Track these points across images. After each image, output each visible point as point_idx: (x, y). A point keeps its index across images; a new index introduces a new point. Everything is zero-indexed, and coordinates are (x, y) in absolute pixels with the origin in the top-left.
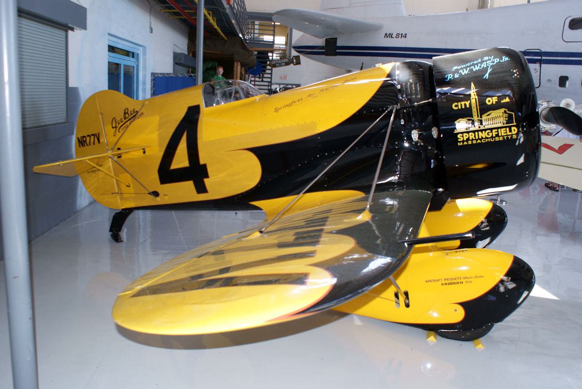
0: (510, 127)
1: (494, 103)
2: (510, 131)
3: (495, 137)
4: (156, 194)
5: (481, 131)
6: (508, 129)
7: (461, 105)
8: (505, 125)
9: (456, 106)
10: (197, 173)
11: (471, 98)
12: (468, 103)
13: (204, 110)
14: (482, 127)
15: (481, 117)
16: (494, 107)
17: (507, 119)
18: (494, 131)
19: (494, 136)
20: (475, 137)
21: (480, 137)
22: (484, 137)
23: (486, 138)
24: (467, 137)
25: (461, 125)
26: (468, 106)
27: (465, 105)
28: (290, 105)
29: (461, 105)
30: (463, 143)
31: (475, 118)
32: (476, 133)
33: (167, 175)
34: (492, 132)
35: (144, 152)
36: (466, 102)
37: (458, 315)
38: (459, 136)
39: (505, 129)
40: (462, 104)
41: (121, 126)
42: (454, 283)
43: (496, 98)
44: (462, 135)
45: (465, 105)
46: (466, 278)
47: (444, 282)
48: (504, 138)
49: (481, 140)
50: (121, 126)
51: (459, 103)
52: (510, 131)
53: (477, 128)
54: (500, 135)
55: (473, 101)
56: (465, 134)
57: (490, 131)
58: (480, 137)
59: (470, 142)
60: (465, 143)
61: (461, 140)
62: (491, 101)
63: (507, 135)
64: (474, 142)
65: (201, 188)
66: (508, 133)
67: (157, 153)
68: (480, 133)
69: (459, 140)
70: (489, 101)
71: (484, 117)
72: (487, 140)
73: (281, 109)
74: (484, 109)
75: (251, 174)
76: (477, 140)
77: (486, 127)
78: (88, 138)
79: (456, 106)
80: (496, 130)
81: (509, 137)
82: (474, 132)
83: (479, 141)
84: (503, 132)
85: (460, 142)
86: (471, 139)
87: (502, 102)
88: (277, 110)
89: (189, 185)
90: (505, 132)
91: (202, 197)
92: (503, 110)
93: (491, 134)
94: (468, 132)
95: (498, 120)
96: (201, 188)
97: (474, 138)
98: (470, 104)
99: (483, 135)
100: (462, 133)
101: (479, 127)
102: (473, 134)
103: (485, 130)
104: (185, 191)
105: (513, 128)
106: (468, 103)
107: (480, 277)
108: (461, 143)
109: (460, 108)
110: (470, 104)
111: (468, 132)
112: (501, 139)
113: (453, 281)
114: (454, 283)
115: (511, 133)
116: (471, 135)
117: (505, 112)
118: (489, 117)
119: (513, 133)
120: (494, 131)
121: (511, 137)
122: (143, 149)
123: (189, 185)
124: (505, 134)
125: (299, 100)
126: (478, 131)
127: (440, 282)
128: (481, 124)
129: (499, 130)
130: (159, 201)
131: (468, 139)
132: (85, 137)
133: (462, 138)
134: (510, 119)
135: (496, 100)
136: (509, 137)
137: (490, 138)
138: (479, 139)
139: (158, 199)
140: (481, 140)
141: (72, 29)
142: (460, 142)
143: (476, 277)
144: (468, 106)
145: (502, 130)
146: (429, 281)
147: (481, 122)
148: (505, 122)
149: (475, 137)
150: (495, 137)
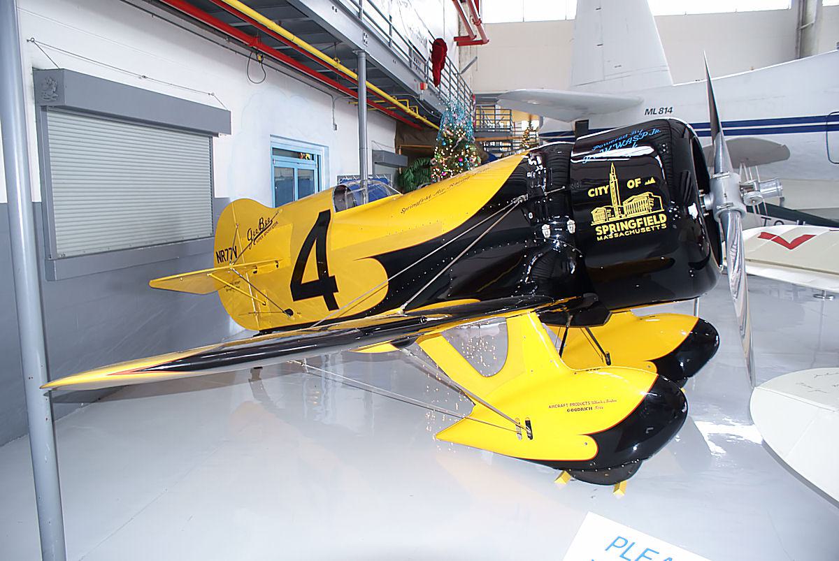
0: (657, 215)
1: (637, 186)
2: (658, 219)
3: (640, 228)
4: (289, 312)
5: (623, 221)
6: (654, 217)
7: (598, 191)
8: (651, 212)
9: (592, 193)
10: (326, 287)
11: (610, 182)
12: (606, 189)
13: (335, 216)
14: (624, 217)
15: (622, 204)
16: (637, 191)
17: (653, 205)
18: (638, 220)
19: (639, 226)
20: (616, 229)
21: (623, 230)
22: (627, 228)
23: (632, 230)
24: (607, 230)
25: (599, 215)
26: (606, 192)
27: (603, 190)
28: (418, 204)
29: (598, 191)
30: (603, 238)
31: (615, 206)
32: (617, 224)
33: (300, 290)
34: (636, 222)
35: (277, 266)
36: (604, 187)
37: (589, 451)
38: (597, 229)
39: (651, 217)
40: (599, 191)
41: (257, 237)
42: (582, 409)
43: (639, 179)
44: (600, 227)
45: (603, 190)
46: (596, 403)
47: (570, 408)
48: (651, 229)
49: (623, 232)
50: (257, 237)
51: (596, 189)
52: (658, 219)
53: (617, 218)
54: (646, 225)
55: (612, 185)
57: (633, 221)
59: (611, 236)
60: (606, 237)
61: (601, 234)
62: (633, 183)
63: (655, 225)
64: (616, 235)
65: (332, 305)
66: (656, 222)
67: (289, 264)
68: (621, 223)
69: (598, 234)
70: (631, 184)
71: (626, 204)
72: (631, 232)
73: (407, 209)
74: (625, 193)
75: (377, 283)
76: (619, 233)
77: (628, 217)
78: (226, 252)
79: (592, 193)
80: (641, 219)
81: (658, 226)
82: (614, 223)
83: (621, 234)
84: (649, 221)
85: (599, 236)
87: (646, 183)
88: (403, 211)
89: (321, 299)
90: (652, 220)
91: (334, 314)
92: (647, 194)
93: (634, 224)
94: (607, 224)
95: (642, 207)
96: (332, 305)
97: (615, 231)
98: (609, 190)
99: (626, 226)
100: (601, 225)
101: (621, 217)
102: (613, 225)
103: (628, 220)
104: (315, 308)
105: (661, 216)
106: (606, 189)
107: (612, 401)
109: (597, 195)
110: (609, 190)
111: (607, 224)
113: (580, 407)
114: (582, 409)
115: (659, 222)
116: (612, 228)
117: (650, 196)
118: (631, 203)
119: (662, 221)
120: (638, 220)
121: (660, 227)
122: (277, 262)
123: (321, 299)
124: (653, 224)
125: (427, 198)
126: (619, 221)
127: (565, 408)
128: (623, 213)
130: (293, 320)
131: (608, 233)
132: (222, 251)
133: (601, 231)
134: (656, 206)
135: (640, 183)
136: (658, 226)
138: (621, 231)
139: (292, 317)
140: (623, 232)
141: (217, 135)
142: (599, 236)
143: (607, 401)
144: (606, 192)
145: (648, 218)
146: (553, 406)
148: (651, 208)
149: (616, 229)
150: (640, 228)
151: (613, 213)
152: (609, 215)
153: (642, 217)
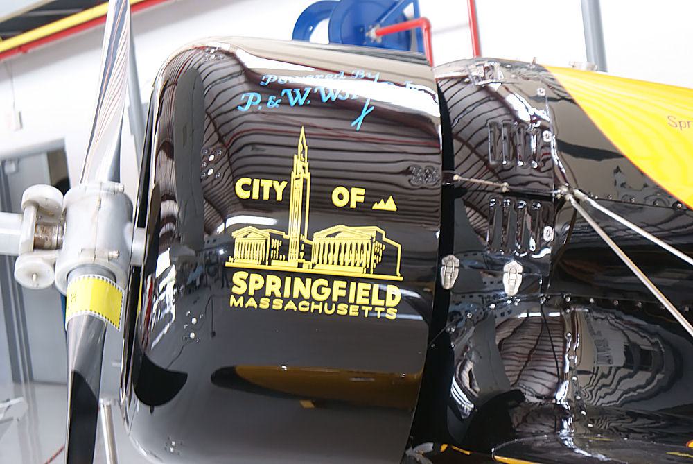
1: (353, 205)
7: (261, 188)
15: (310, 238)
19: (335, 298)
20: (282, 290)
21: (296, 295)
22: (307, 296)
26: (279, 198)
27: (272, 189)
29: (261, 188)
36: (276, 183)
43: (362, 191)
44: (245, 275)
45: (272, 189)
51: (256, 182)
53: (291, 265)
54: (351, 300)
55: (297, 187)
56: (254, 277)
57: (325, 282)
58: (296, 295)
59: (264, 303)
60: (252, 302)
64: (278, 305)
69: (235, 289)
70: (341, 197)
77: (319, 269)
80: (344, 284)
86: (268, 293)
87: (376, 207)
97: (278, 294)
100: (250, 271)
101: (300, 265)
108: (241, 299)
111: (264, 273)
112: (354, 311)
118: (331, 241)
120: (337, 284)
128: (308, 256)
129: (353, 285)
137: (324, 302)
142: (237, 297)
144: (279, 198)
147: (307, 251)
151: (284, 250)
152: (274, 254)
153: (349, 279)
